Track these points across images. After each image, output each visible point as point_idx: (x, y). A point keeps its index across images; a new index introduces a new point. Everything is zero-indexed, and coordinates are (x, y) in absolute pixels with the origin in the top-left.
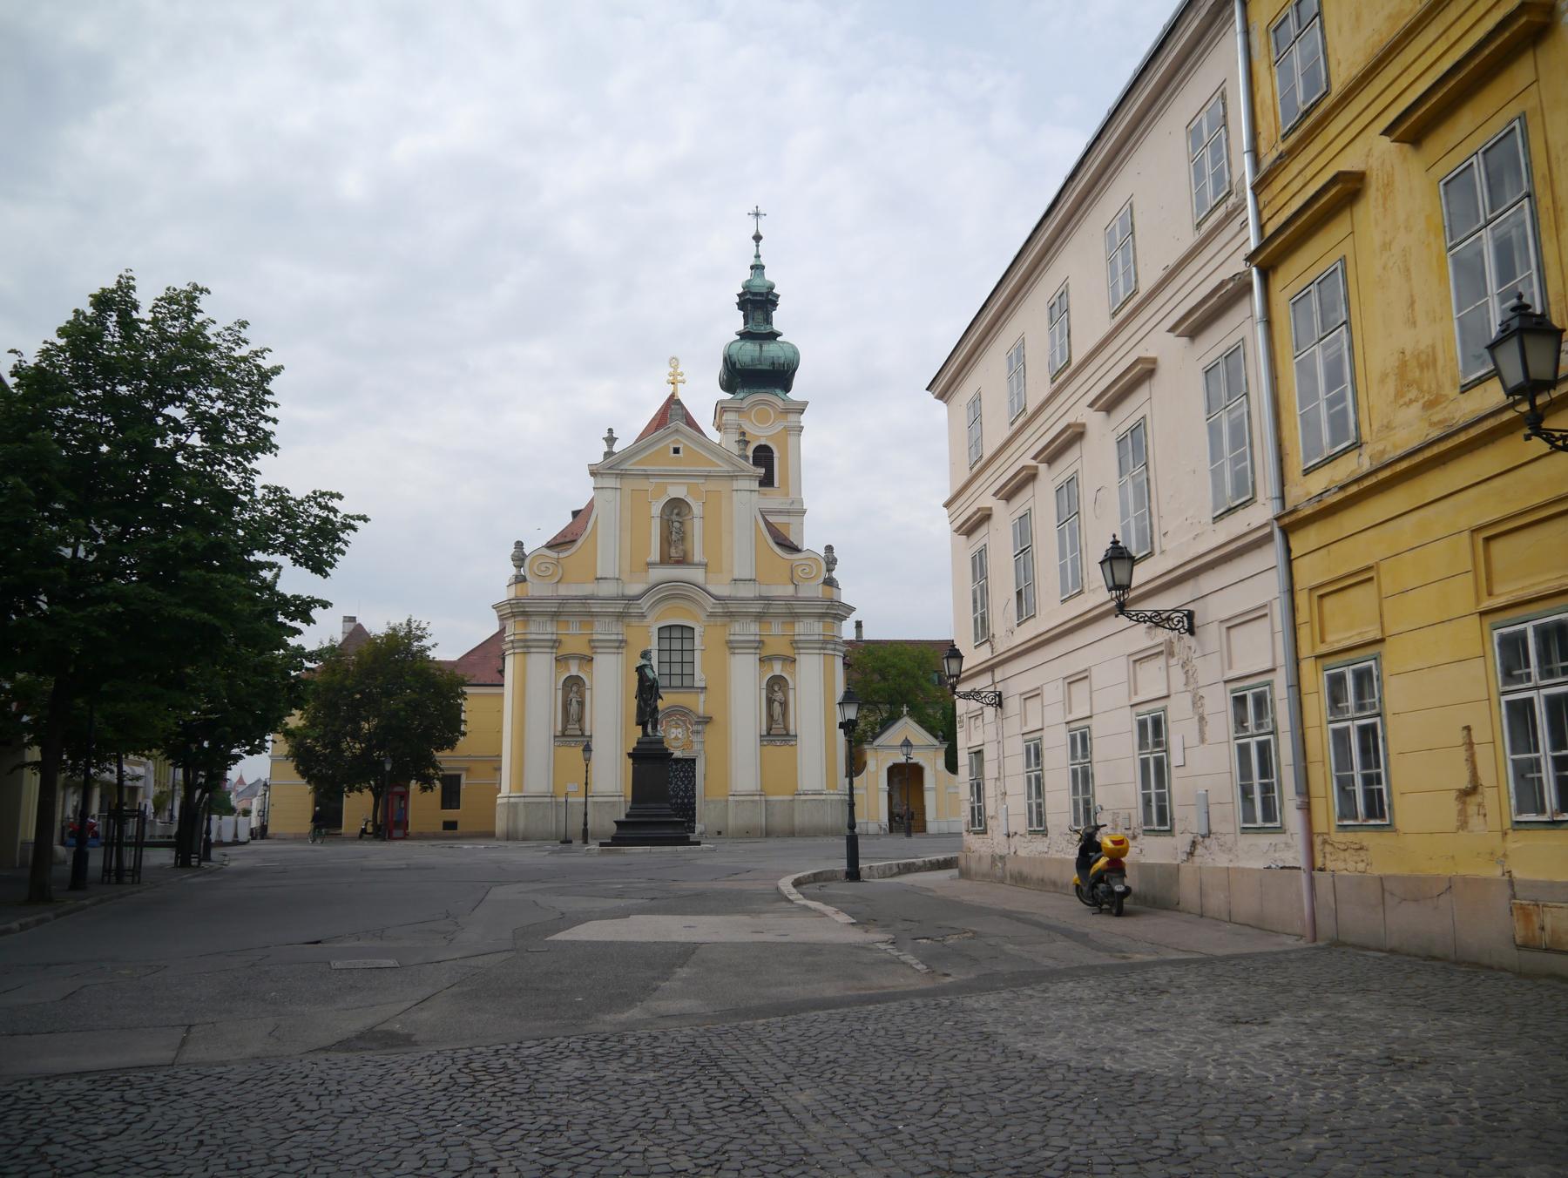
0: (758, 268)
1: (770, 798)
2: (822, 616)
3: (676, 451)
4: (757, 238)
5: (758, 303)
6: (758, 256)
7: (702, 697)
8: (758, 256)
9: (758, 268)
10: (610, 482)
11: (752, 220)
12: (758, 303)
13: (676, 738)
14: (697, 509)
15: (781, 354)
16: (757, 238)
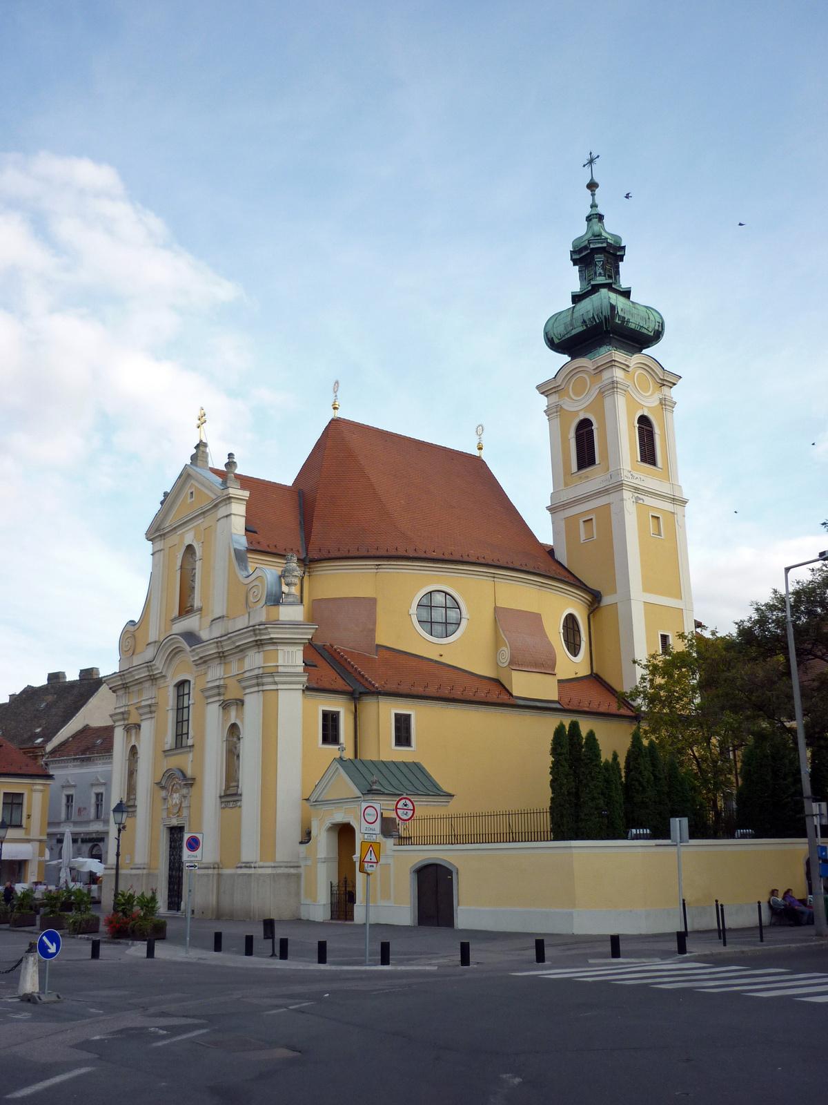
0: (595, 217)
1: (222, 871)
2: (259, 644)
3: (192, 493)
4: (592, 186)
5: (598, 257)
6: (594, 206)
7: (191, 755)
8: (594, 206)
9: (595, 217)
10: (160, 545)
11: (587, 169)
13: (176, 804)
14: (199, 552)
15: (589, 307)
16: (592, 186)
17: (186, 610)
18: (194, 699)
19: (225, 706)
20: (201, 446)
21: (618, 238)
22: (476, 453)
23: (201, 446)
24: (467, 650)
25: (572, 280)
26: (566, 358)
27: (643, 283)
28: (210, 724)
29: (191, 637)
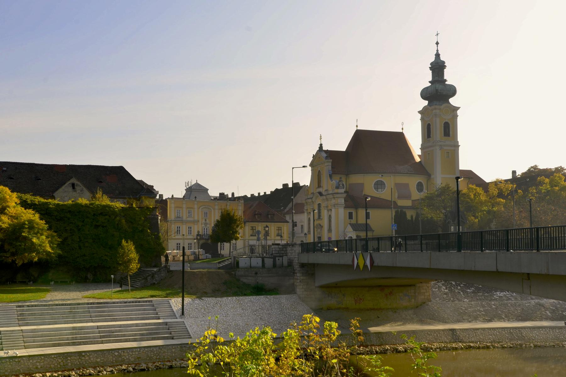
0: (438, 55)
4: (437, 43)
5: (438, 67)
6: (437, 51)
8: (437, 51)
9: (438, 55)
12: (438, 67)
16: (437, 43)
17: (319, 186)
18: (322, 208)
19: (328, 210)
20: (321, 145)
21: (444, 62)
22: (401, 131)
23: (321, 145)
24: (384, 194)
25: (429, 76)
26: (426, 103)
27: (450, 77)
28: (325, 213)
29: (320, 194)
